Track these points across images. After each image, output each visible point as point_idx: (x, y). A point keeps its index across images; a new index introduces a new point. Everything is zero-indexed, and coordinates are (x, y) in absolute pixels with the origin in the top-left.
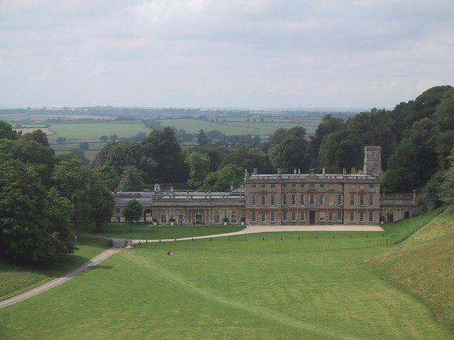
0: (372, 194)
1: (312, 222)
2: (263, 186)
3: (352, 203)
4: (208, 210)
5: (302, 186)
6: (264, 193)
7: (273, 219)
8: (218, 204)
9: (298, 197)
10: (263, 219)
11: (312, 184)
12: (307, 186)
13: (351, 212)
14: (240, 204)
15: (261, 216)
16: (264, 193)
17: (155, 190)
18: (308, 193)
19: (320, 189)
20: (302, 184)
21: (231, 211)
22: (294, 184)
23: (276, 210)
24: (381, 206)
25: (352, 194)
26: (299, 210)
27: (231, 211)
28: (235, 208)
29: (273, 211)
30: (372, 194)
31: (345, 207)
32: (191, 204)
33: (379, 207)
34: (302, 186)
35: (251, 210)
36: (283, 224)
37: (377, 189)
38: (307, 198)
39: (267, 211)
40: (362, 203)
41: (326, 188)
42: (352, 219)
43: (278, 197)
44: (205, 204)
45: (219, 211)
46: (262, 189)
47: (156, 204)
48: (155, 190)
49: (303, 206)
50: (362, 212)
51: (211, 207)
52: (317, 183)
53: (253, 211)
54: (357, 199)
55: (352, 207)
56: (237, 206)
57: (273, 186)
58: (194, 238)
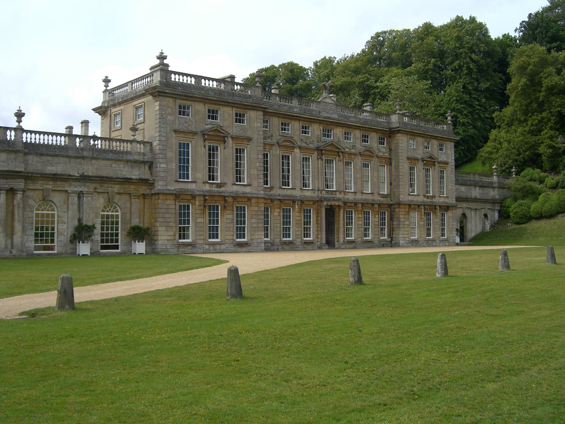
1: (330, 244)
2: (213, 115)
6: (217, 136)
7: (240, 233)
8: (51, 169)
12: (315, 130)
14: (135, 173)
15: (204, 220)
16: (217, 136)
18: (320, 151)
19: (346, 144)
21: (101, 201)
23: (249, 199)
24: (459, 199)
33: (452, 201)
35: (177, 195)
37: (448, 154)
45: (57, 198)
46: (209, 124)
51: (28, 177)
56: (127, 181)
57: (239, 119)
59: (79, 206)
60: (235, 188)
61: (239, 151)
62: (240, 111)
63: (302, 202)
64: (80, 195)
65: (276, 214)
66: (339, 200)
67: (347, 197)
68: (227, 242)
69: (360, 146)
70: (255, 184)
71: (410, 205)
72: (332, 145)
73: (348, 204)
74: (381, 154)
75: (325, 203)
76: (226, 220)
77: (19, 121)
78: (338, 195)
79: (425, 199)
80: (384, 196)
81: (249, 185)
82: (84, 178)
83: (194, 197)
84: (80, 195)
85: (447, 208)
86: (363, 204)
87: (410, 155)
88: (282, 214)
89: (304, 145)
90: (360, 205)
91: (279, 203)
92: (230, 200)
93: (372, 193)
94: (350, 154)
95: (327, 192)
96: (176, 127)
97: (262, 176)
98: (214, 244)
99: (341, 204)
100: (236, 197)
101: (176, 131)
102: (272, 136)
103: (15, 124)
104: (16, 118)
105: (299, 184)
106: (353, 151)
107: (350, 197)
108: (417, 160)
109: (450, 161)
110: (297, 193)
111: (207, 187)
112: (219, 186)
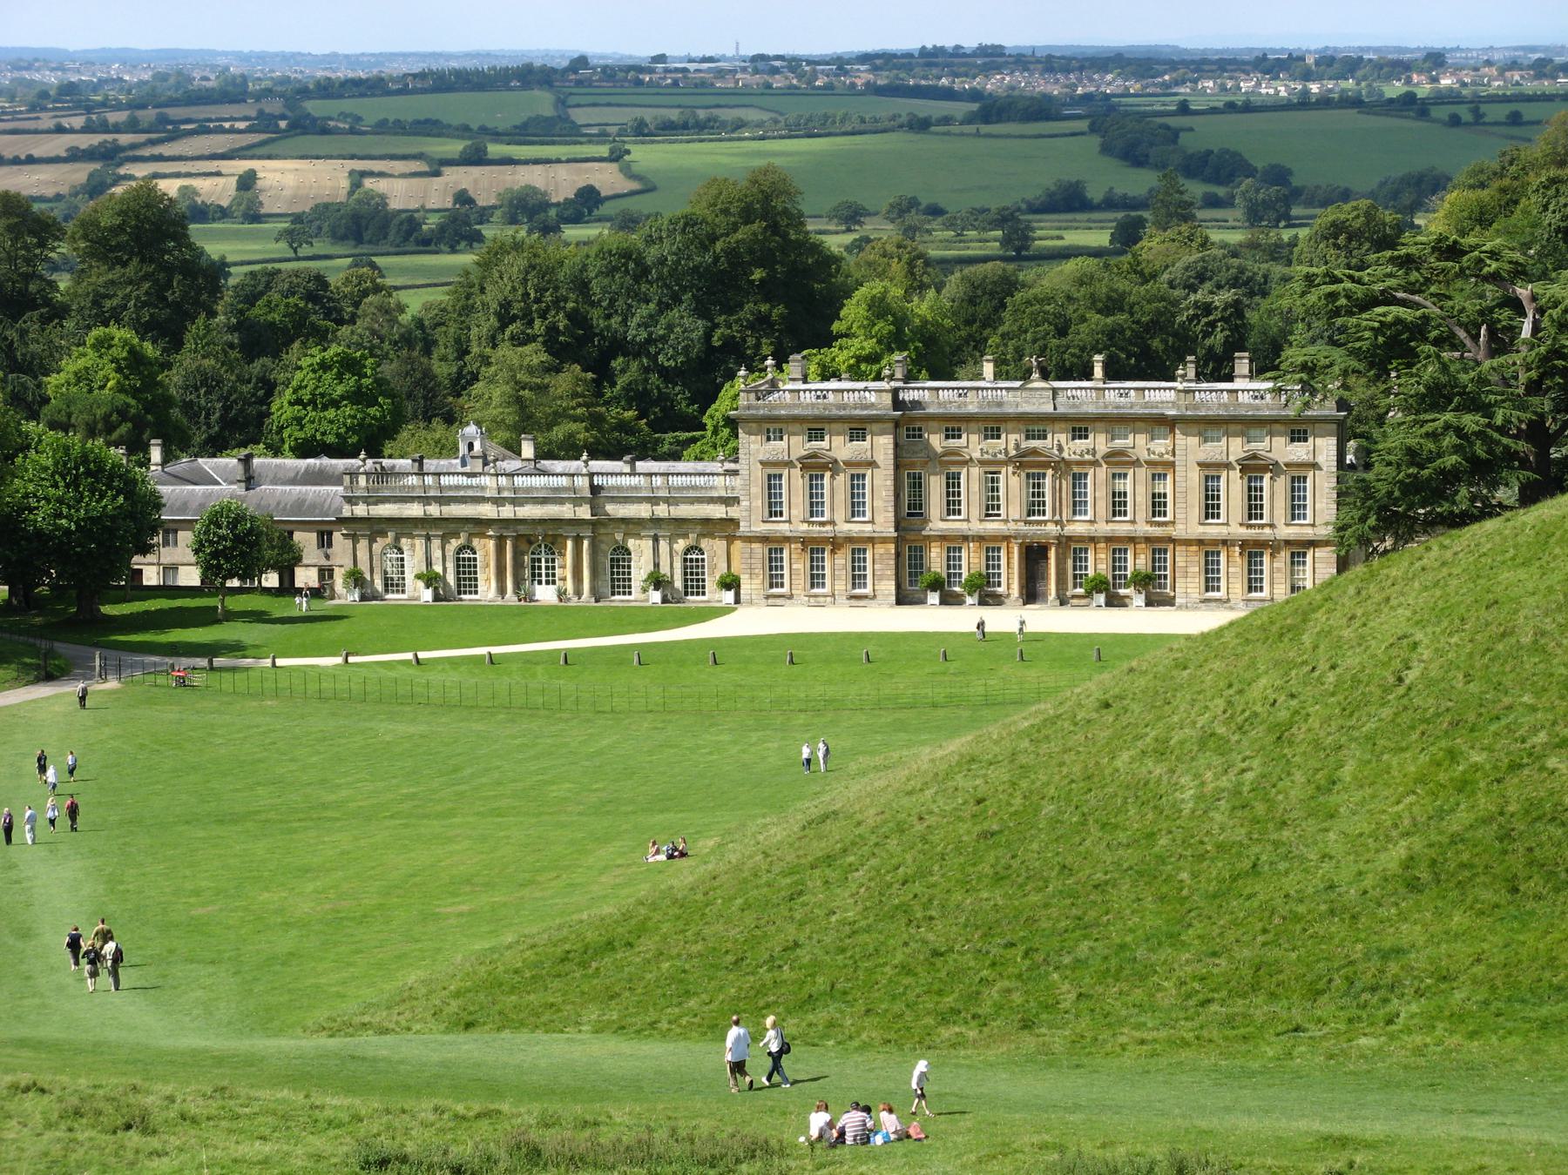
0: (1298, 475)
3: (1211, 509)
4: (578, 541)
9: (972, 482)
10: (816, 580)
11: (1035, 425)
13: (1210, 550)
14: (718, 511)
16: (815, 467)
17: (463, 449)
19: (1074, 448)
20: (992, 426)
22: (954, 425)
25: (1211, 471)
26: (980, 538)
27: (681, 545)
29: (857, 546)
30: (1298, 475)
31: (1178, 531)
32: (507, 512)
35: (764, 539)
38: (1012, 484)
39: (836, 543)
40: (1254, 509)
41: (1099, 442)
42: (1210, 584)
43: (880, 484)
44: (566, 511)
47: (360, 510)
48: (463, 449)
49: (992, 527)
50: (1253, 551)
53: (774, 545)
54: (1233, 488)
55: (1213, 531)
58: (495, 650)
59: (656, 550)
64: (656, 539)
66: (1047, 535)
70: (879, 519)
71: (1200, 542)
72: (1034, 452)
76: (836, 565)
78: (1051, 527)
79: (1243, 530)
80: (1159, 524)
81: (872, 522)
82: (656, 521)
84: (656, 539)
85: (1313, 544)
87: (1202, 457)
88: (945, 555)
93: (1133, 522)
95: (1030, 523)
96: (761, 457)
98: (816, 596)
100: (850, 539)
105: (976, 512)
106: (1088, 457)
107: (1078, 528)
108: (1228, 466)
109: (1320, 459)
112: (822, 524)
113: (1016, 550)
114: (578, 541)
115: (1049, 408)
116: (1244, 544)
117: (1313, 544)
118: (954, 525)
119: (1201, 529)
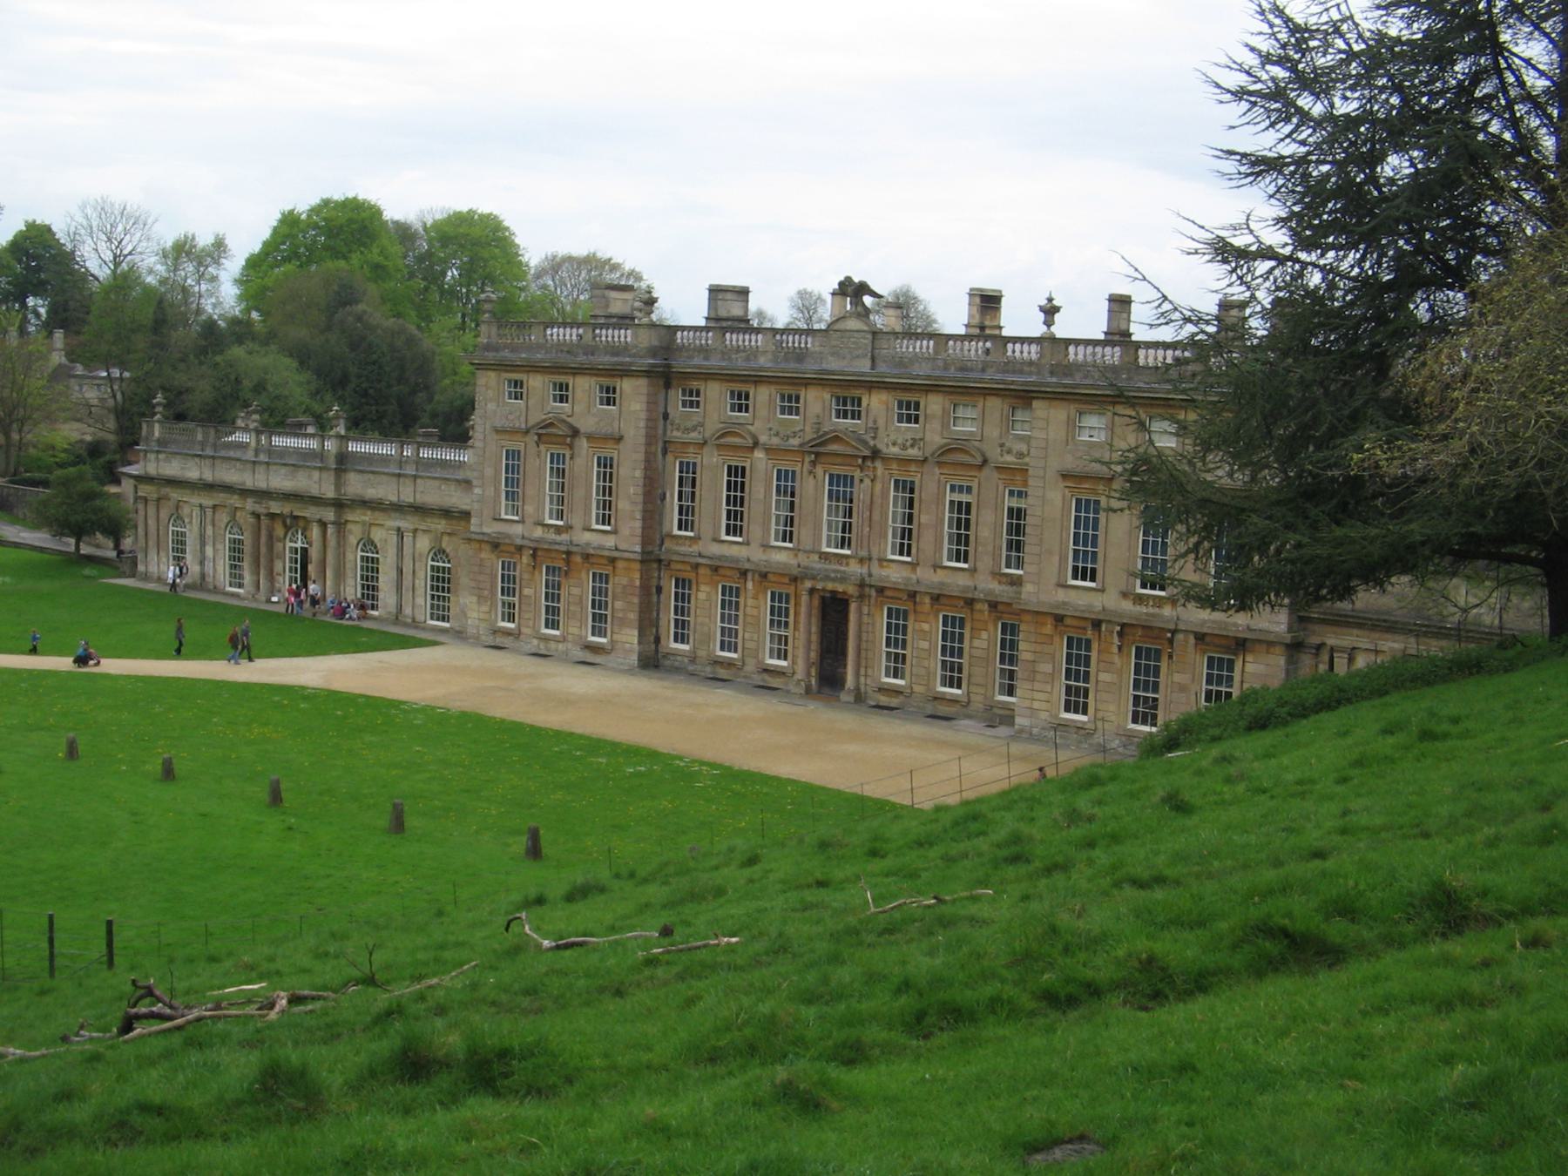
5: (791, 404)
12: (816, 402)
19: (894, 435)
27: (424, 543)
28: (441, 525)
34: (791, 404)
35: (495, 546)
36: (652, 661)
45: (377, 535)
52: (872, 386)
55: (1082, 597)
60: (587, 537)
61: (606, 463)
62: (606, 381)
63: (764, 576)
64: (400, 533)
65: (702, 596)
66: (843, 579)
67: (884, 572)
68: (570, 638)
69: (935, 438)
70: (625, 531)
71: (1059, 619)
73: (888, 593)
74: (1009, 458)
75: (808, 584)
77: (1049, 323)
79: (1127, 605)
82: (398, 508)
83: (520, 549)
85: (1241, 645)
86: (936, 598)
87: (1070, 463)
89: (775, 441)
90: (927, 600)
91: (708, 572)
92: (578, 559)
94: (905, 462)
97: (638, 516)
99: (852, 590)
101: (497, 431)
102: (702, 425)
103: (1037, 330)
104: (1042, 316)
110: (756, 555)
111: (538, 532)
113: (804, 599)
114: (323, 525)
115: (864, 366)
116: (1125, 629)
117: (1241, 645)
118: (732, 548)
119: (1061, 595)
